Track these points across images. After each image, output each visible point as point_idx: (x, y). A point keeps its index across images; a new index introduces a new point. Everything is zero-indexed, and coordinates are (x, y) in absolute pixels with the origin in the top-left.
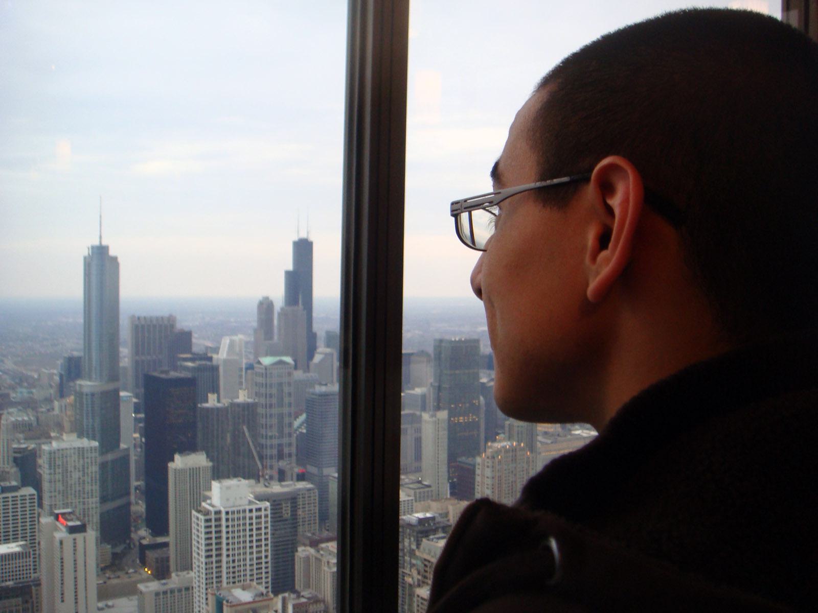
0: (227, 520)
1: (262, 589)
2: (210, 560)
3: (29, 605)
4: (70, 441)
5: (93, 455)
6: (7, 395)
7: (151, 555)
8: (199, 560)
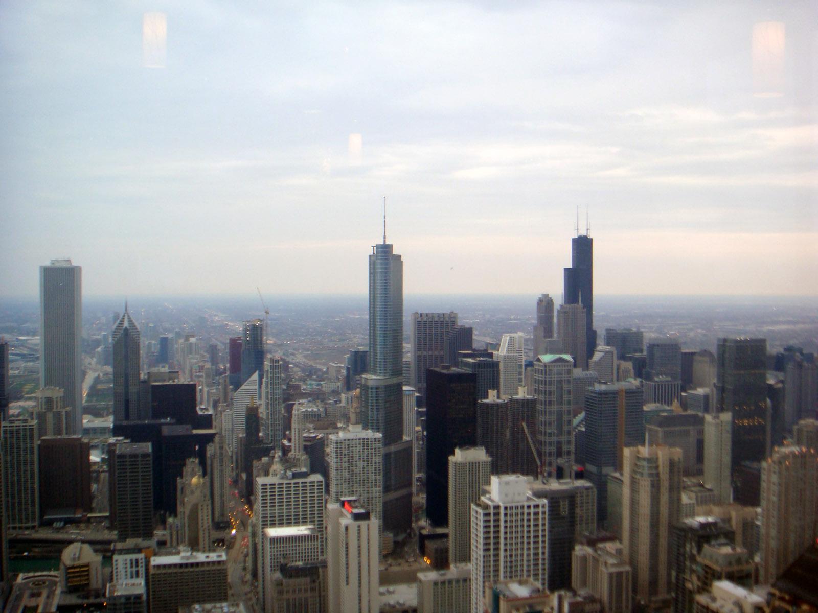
0: (506, 515)
1: (538, 585)
2: (488, 553)
3: (317, 584)
4: (355, 432)
6: (299, 386)
7: (430, 545)
8: (477, 553)
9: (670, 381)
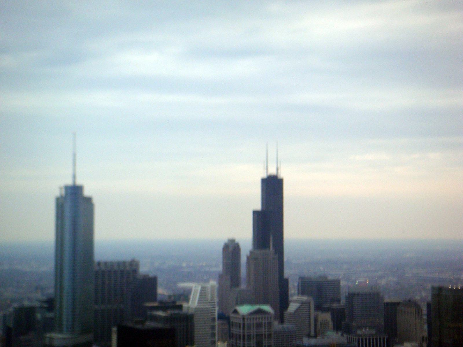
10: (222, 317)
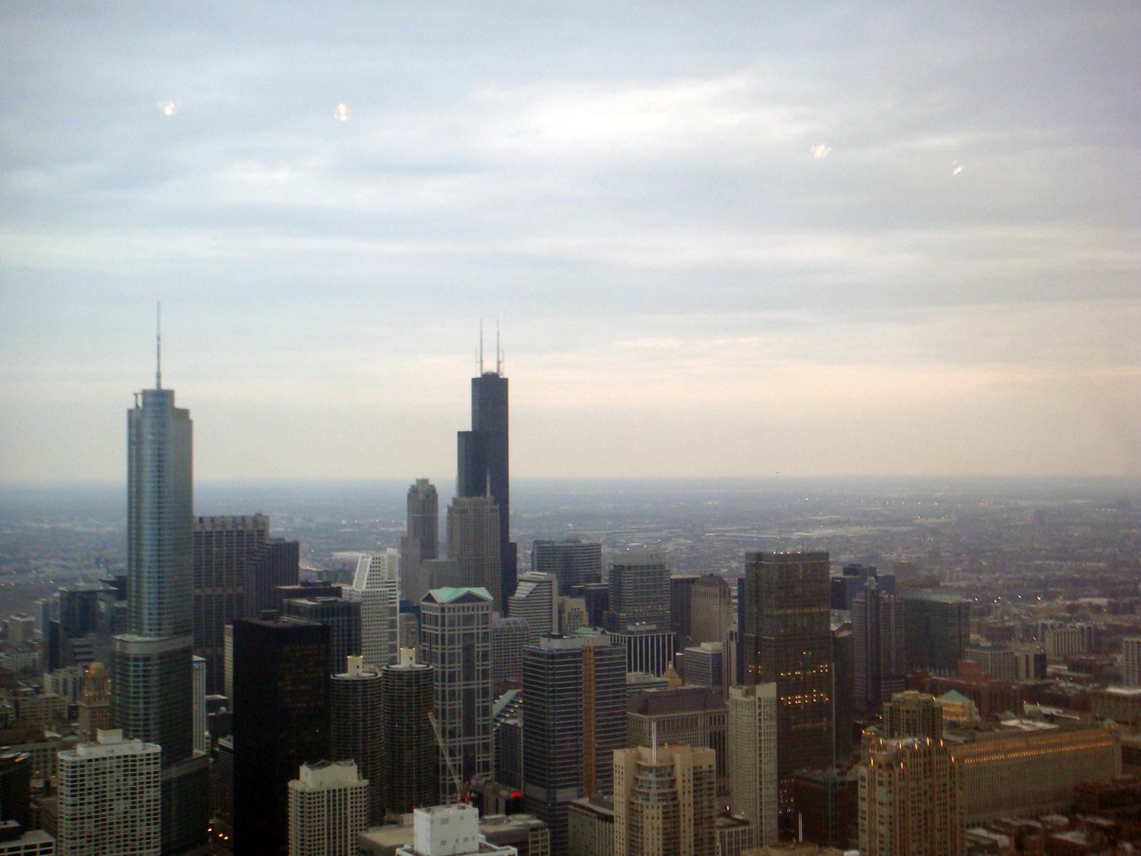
5: (152, 768)
9: (655, 631)
10: (406, 607)
